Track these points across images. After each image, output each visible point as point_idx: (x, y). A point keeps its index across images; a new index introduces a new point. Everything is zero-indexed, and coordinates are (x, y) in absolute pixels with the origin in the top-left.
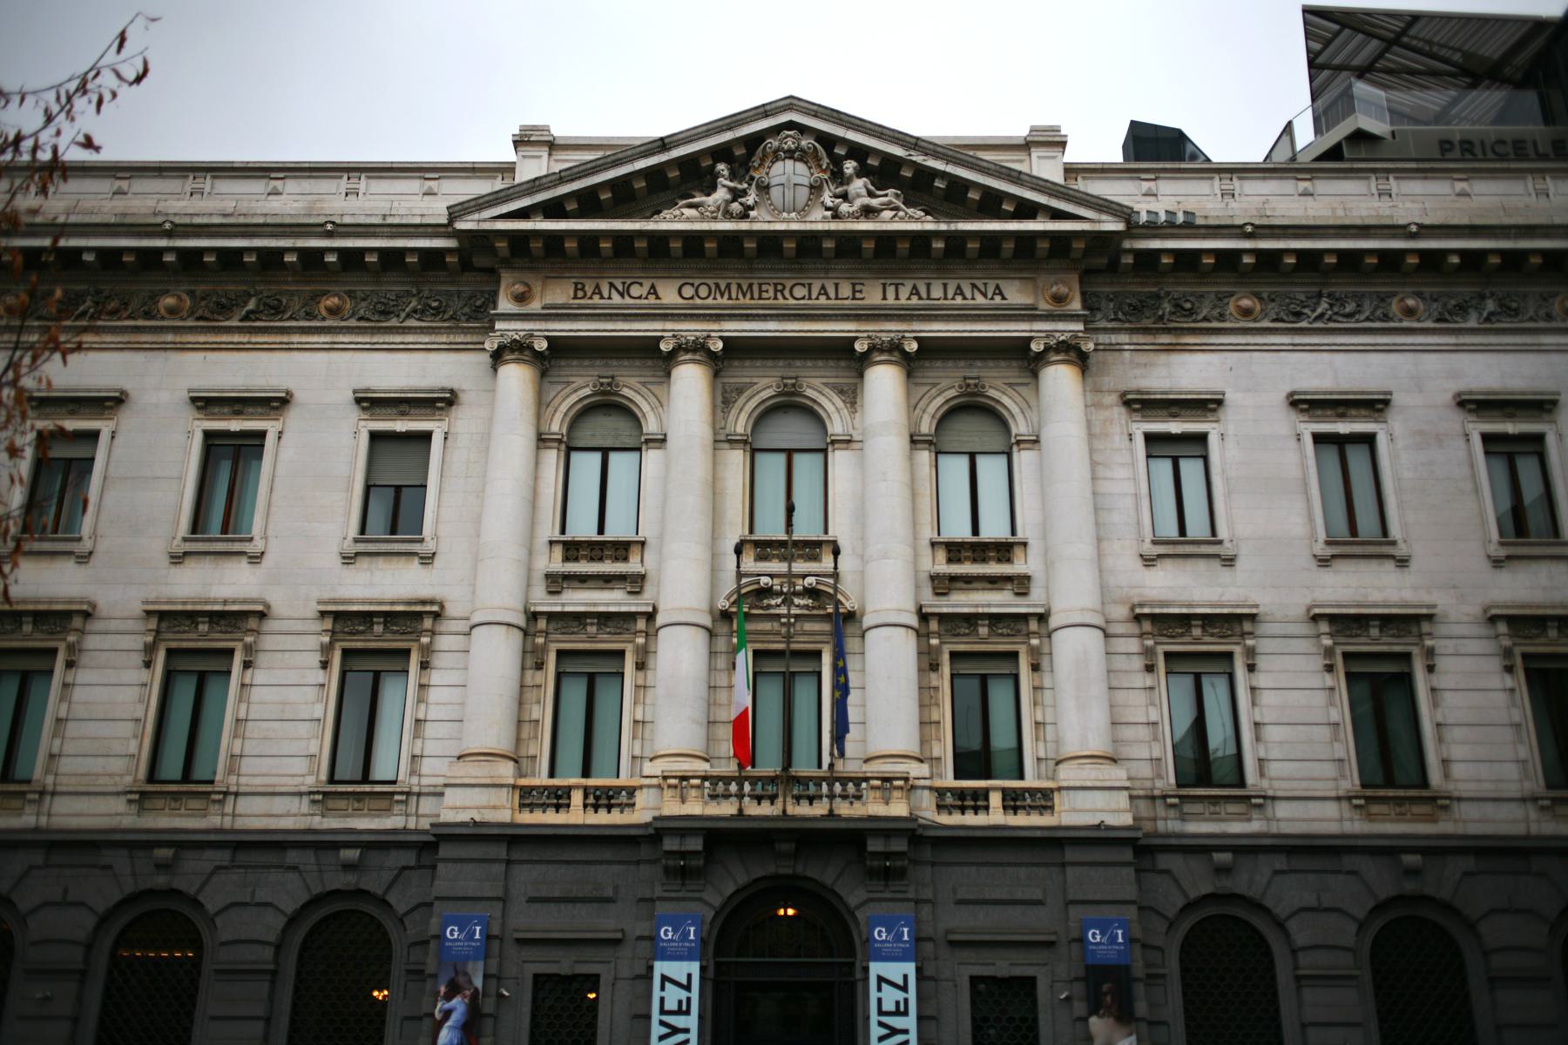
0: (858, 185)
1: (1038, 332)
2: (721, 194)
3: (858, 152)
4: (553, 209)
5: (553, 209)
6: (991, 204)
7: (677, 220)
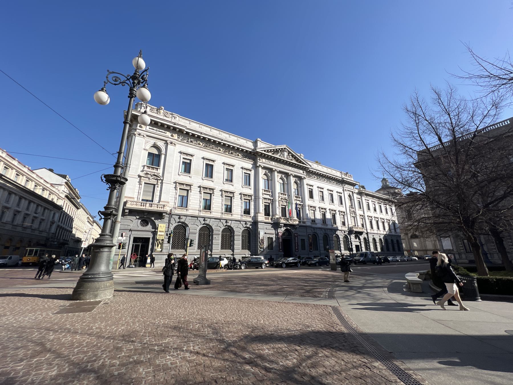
1: (303, 176)
4: (265, 151)
5: (265, 151)
6: (300, 162)
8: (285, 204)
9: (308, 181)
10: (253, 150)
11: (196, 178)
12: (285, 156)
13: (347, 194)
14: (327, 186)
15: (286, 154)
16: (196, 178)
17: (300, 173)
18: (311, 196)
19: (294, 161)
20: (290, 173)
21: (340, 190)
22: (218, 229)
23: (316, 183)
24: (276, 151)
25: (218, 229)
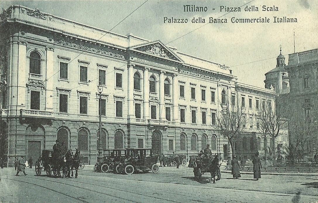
0: (163, 52)
2: (152, 50)
3: (164, 48)
4: (137, 49)
5: (137, 49)
6: (173, 57)
7: (148, 53)
8: (155, 104)
9: (180, 77)
10: (127, 48)
11: (74, 83)
12: (156, 52)
13: (220, 90)
14: (199, 82)
15: (158, 49)
16: (74, 83)
17: (173, 69)
18: (182, 95)
19: (167, 58)
20: (162, 70)
21: (214, 85)
22: (93, 130)
23: (188, 80)
24: (149, 47)
25: (93, 130)
